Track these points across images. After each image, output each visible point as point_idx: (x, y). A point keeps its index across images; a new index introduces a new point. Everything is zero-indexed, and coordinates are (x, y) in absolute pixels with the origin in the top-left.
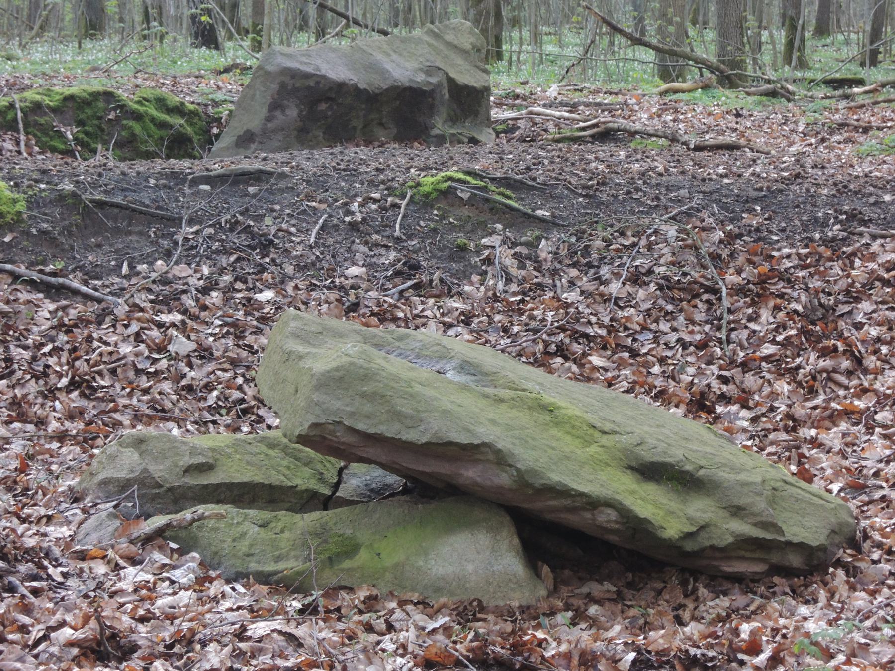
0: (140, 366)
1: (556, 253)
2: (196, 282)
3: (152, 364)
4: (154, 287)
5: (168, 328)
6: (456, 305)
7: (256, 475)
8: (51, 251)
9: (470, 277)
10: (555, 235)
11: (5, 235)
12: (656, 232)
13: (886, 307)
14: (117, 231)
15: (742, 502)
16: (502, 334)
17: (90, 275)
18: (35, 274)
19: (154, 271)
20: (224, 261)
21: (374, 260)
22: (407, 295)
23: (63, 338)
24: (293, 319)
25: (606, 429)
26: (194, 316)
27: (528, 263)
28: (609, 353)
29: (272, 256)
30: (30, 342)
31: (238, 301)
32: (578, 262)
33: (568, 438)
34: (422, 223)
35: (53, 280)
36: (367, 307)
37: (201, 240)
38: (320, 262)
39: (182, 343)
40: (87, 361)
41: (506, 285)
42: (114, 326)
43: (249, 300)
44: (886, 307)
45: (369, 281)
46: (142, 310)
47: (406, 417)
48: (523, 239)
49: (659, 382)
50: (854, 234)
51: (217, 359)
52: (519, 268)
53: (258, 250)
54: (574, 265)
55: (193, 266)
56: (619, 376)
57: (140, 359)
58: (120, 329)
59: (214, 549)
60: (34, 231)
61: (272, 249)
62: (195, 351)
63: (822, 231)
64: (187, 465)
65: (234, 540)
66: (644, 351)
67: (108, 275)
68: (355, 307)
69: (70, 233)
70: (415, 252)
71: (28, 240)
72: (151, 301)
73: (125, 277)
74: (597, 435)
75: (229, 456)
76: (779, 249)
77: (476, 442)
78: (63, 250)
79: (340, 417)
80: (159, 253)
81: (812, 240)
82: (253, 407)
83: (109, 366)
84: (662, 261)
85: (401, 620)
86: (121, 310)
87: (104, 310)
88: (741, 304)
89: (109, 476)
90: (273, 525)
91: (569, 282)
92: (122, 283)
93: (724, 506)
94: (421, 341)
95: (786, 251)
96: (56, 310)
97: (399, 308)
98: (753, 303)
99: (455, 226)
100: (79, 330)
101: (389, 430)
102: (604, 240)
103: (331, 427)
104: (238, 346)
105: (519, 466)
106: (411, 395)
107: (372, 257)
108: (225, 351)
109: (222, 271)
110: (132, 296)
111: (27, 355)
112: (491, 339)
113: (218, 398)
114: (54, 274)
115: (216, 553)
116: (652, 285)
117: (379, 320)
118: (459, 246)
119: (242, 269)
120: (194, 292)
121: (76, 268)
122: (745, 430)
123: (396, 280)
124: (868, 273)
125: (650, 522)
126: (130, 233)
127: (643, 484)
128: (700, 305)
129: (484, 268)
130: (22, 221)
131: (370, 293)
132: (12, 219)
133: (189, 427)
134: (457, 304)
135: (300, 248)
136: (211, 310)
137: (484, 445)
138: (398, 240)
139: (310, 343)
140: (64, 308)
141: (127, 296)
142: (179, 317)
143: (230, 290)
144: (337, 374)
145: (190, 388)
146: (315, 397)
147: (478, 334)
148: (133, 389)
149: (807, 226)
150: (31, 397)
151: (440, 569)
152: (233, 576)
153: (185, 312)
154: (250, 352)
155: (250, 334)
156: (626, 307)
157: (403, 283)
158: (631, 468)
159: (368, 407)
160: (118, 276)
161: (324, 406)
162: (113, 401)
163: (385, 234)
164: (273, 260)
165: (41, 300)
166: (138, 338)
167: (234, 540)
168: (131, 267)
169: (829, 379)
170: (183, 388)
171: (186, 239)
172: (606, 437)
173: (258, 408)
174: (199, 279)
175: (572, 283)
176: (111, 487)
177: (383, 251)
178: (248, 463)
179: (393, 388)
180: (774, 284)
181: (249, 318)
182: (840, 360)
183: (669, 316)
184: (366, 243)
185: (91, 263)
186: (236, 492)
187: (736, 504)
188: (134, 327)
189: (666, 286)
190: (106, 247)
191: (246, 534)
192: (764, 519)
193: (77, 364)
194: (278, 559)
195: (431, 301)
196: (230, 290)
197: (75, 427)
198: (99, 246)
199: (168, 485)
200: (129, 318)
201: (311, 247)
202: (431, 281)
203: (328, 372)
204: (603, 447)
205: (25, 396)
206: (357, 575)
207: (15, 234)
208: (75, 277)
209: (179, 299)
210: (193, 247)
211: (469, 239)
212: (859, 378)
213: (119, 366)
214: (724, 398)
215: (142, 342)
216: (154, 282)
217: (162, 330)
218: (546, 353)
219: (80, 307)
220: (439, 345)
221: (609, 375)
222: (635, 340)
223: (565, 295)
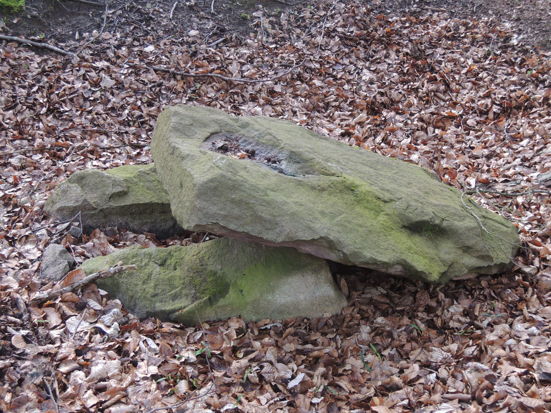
0: (86, 96)
1: (289, 21)
2: (114, 42)
3: (92, 94)
4: (92, 46)
5: (100, 71)
6: (245, 51)
7: (153, 197)
8: (38, 27)
9: (249, 34)
10: (288, 10)
11: (13, 19)
12: (334, 8)
13: (449, 51)
14: (73, 14)
15: (470, 243)
16: (269, 68)
17: (60, 39)
18: (30, 41)
19: (92, 36)
20: (128, 29)
21: (202, 26)
22: (220, 45)
23: (45, 79)
24: (174, 115)
25: (386, 199)
26: (114, 62)
27: (276, 26)
28: (322, 78)
29: (152, 26)
30: (27, 83)
31: (136, 53)
32: (300, 25)
33: (366, 213)
34: (224, 5)
35: (39, 44)
36: (201, 53)
37: (115, 18)
38: (176, 28)
39: (107, 81)
40: (58, 95)
41: (267, 38)
42: (72, 71)
43: (141, 52)
44: (449, 51)
45: (201, 38)
46: (86, 61)
47: (265, 221)
48: (273, 13)
49: (349, 95)
50: (423, 9)
51: (126, 89)
52: (272, 29)
53: (144, 23)
54: (298, 27)
55: (112, 33)
56: (329, 92)
57: (86, 90)
58: (75, 72)
59: (130, 293)
60: (29, 16)
61: (152, 22)
62: (115, 84)
63: (409, 8)
64: (111, 193)
65: (144, 283)
66: (339, 76)
67: (68, 40)
68: (195, 54)
69: (48, 16)
70: (222, 21)
71: (26, 22)
72: (91, 55)
73: (77, 40)
74: (382, 204)
75: (136, 184)
76: (392, 18)
77: (316, 237)
78: (44, 26)
79: (217, 219)
80: (94, 25)
81: (404, 12)
82: (147, 121)
83: (69, 97)
84: (339, 25)
85: (268, 373)
86: (76, 60)
87: (66, 60)
88: (380, 48)
89: (63, 205)
90: (168, 262)
91: (297, 36)
92: (75, 44)
93: (460, 246)
94: (257, 130)
95: (394, 18)
96: (41, 62)
97: (217, 54)
98: (386, 48)
99: (240, 6)
100: (53, 74)
101: (254, 230)
102: (311, 13)
103: (211, 227)
104: (137, 80)
105: (345, 251)
106: (268, 203)
107: (201, 24)
108: (131, 84)
109: (126, 36)
110: (81, 52)
111: (24, 92)
112: (264, 71)
113: (128, 115)
114: (40, 41)
115: (132, 297)
116: (336, 37)
117: (208, 62)
118: (242, 18)
119: (137, 33)
120: (113, 48)
121: (52, 36)
122: (401, 129)
123: (214, 37)
124: (438, 32)
125: (424, 273)
126: (79, 15)
127: (412, 237)
128: (361, 49)
129: (255, 29)
130: (23, 11)
131: (202, 46)
132: (18, 10)
133: (113, 138)
134: (244, 51)
135: (165, 20)
136: (122, 59)
137: (321, 238)
138: (213, 15)
139: (186, 135)
140: (45, 61)
141: (79, 52)
142: (106, 64)
143: (130, 47)
144: (211, 184)
145: (113, 109)
146: (198, 203)
147: (258, 69)
148: (82, 111)
149: (401, 5)
150: (26, 120)
151: (283, 299)
152: (145, 316)
153: (108, 60)
154: (144, 84)
155: (143, 73)
156: (325, 50)
157: (218, 40)
158: (404, 227)
159: (236, 211)
160: (74, 40)
161: (205, 211)
162: (71, 121)
163: (206, 11)
164: (152, 28)
165: (33, 56)
166: (84, 77)
167: (144, 283)
168: (80, 35)
169: (435, 95)
170: (109, 109)
171: (108, 17)
172: (387, 205)
173: (150, 120)
174: (115, 40)
175: (298, 37)
176: (65, 212)
177: (206, 21)
178: (148, 188)
179: (254, 197)
180: (394, 37)
181: (142, 63)
182: (439, 85)
183: (348, 55)
184: (198, 17)
185: (60, 33)
186: (141, 208)
187: (467, 245)
188: (82, 71)
189: (344, 38)
190: (67, 23)
191: (151, 274)
192: (483, 254)
193: (52, 96)
194: (175, 297)
195: (233, 50)
196: (130, 47)
197: (49, 141)
198: (64, 23)
199: (100, 208)
200: (80, 66)
201: (171, 20)
202: (231, 38)
203: (206, 183)
204: (387, 214)
205: (23, 120)
206: (229, 309)
207: (19, 18)
208: (51, 42)
209: (106, 52)
210: (112, 22)
211: (247, 13)
212: (449, 95)
213: (74, 97)
214: (384, 105)
215: (87, 80)
216: (92, 43)
217: (97, 72)
218: (292, 79)
219: (54, 60)
220: (271, 135)
221: (325, 91)
222: (333, 70)
223: (296, 44)
